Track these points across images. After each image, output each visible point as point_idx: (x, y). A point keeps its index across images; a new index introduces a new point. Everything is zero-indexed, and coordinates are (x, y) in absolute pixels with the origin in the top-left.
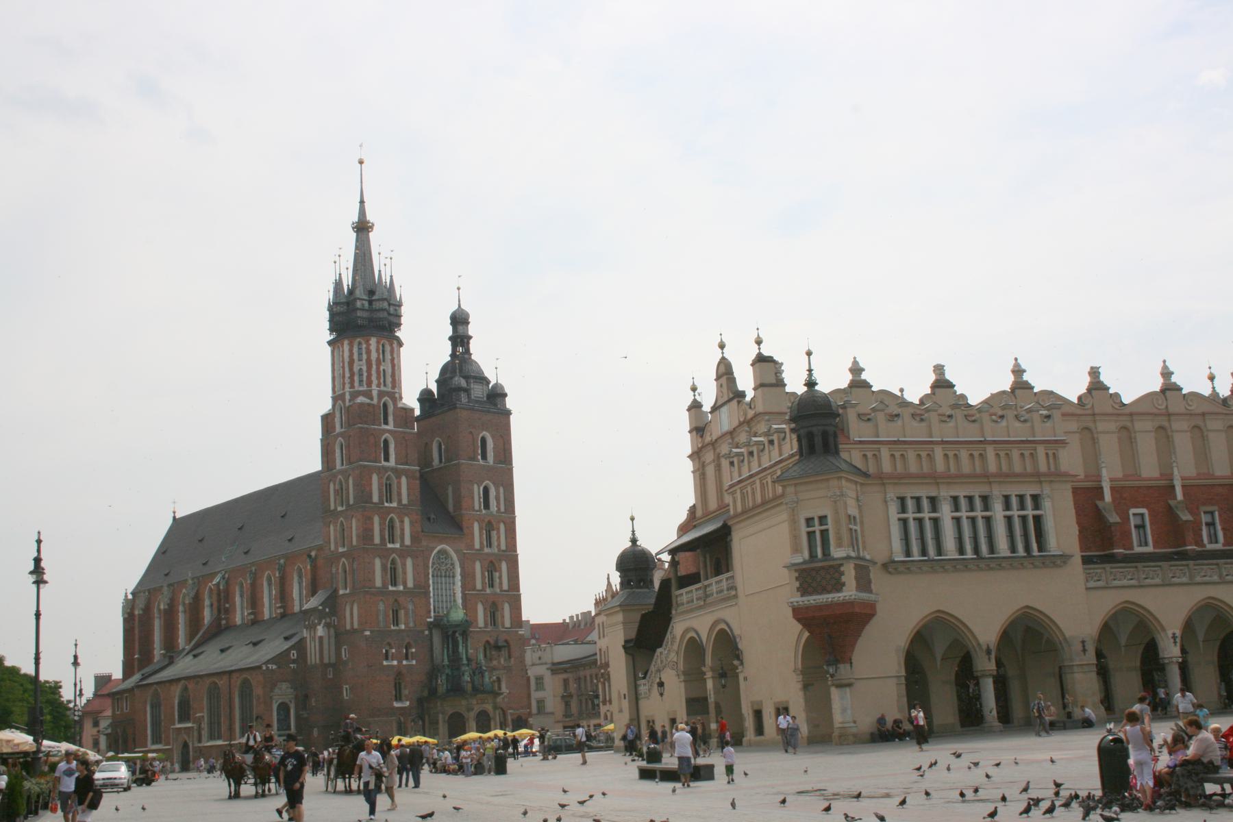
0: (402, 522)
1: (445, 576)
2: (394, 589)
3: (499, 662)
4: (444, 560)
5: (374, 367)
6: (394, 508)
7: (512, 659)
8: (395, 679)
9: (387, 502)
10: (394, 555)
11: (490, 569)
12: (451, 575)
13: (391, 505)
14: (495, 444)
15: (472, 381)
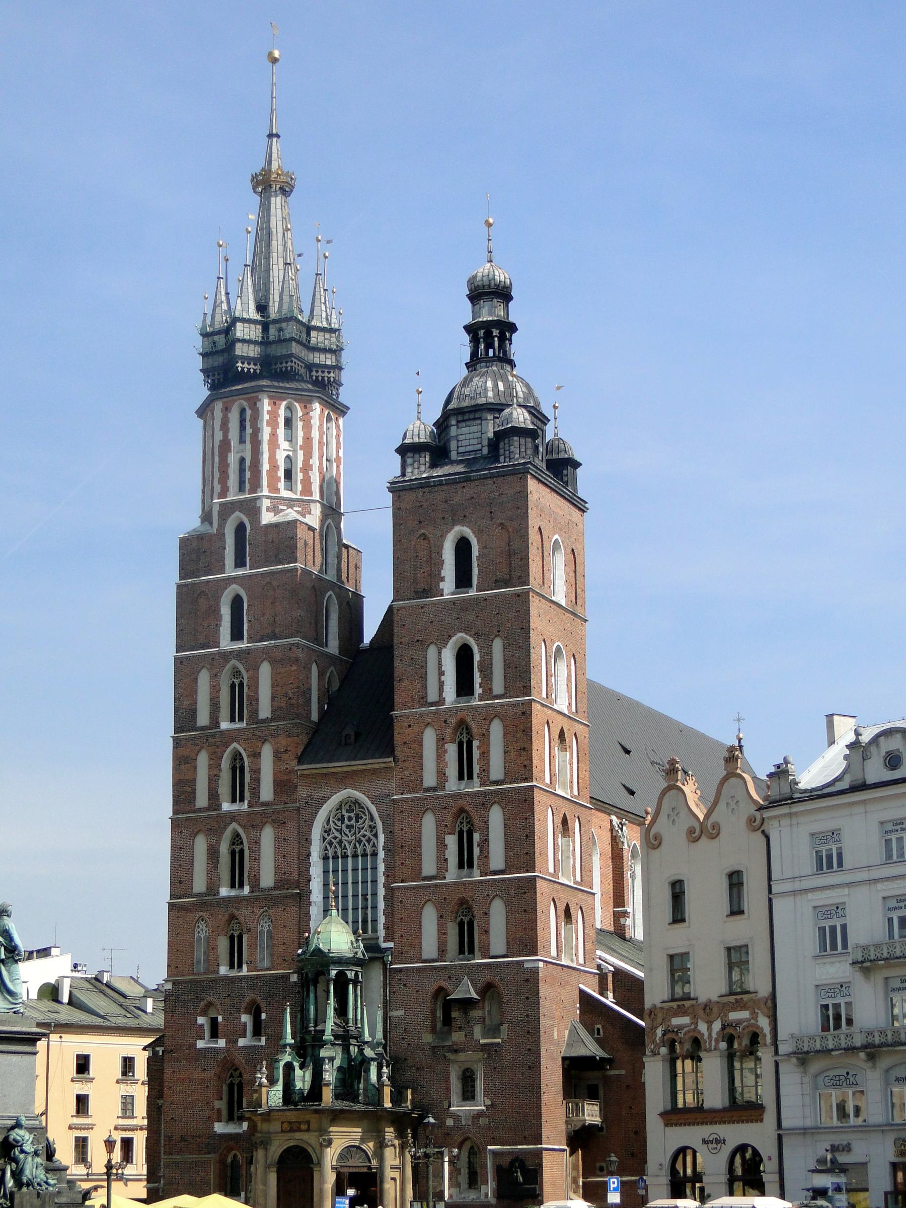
0: (256, 755)
1: (355, 856)
2: (233, 893)
3: (470, 1034)
4: (353, 822)
5: (217, 459)
6: (239, 730)
7: (505, 1026)
8: (231, 1076)
9: (232, 720)
10: (234, 825)
11: (465, 829)
12: (369, 850)
13: (237, 725)
14: (483, 547)
15: (453, 422)
